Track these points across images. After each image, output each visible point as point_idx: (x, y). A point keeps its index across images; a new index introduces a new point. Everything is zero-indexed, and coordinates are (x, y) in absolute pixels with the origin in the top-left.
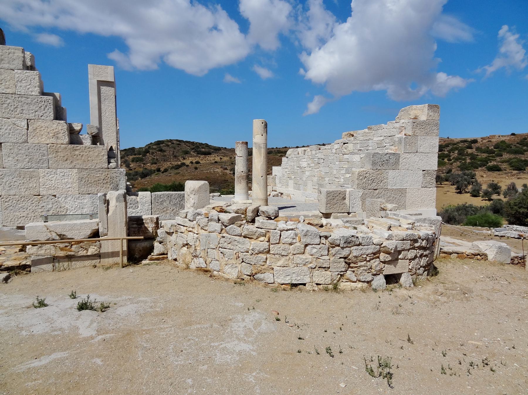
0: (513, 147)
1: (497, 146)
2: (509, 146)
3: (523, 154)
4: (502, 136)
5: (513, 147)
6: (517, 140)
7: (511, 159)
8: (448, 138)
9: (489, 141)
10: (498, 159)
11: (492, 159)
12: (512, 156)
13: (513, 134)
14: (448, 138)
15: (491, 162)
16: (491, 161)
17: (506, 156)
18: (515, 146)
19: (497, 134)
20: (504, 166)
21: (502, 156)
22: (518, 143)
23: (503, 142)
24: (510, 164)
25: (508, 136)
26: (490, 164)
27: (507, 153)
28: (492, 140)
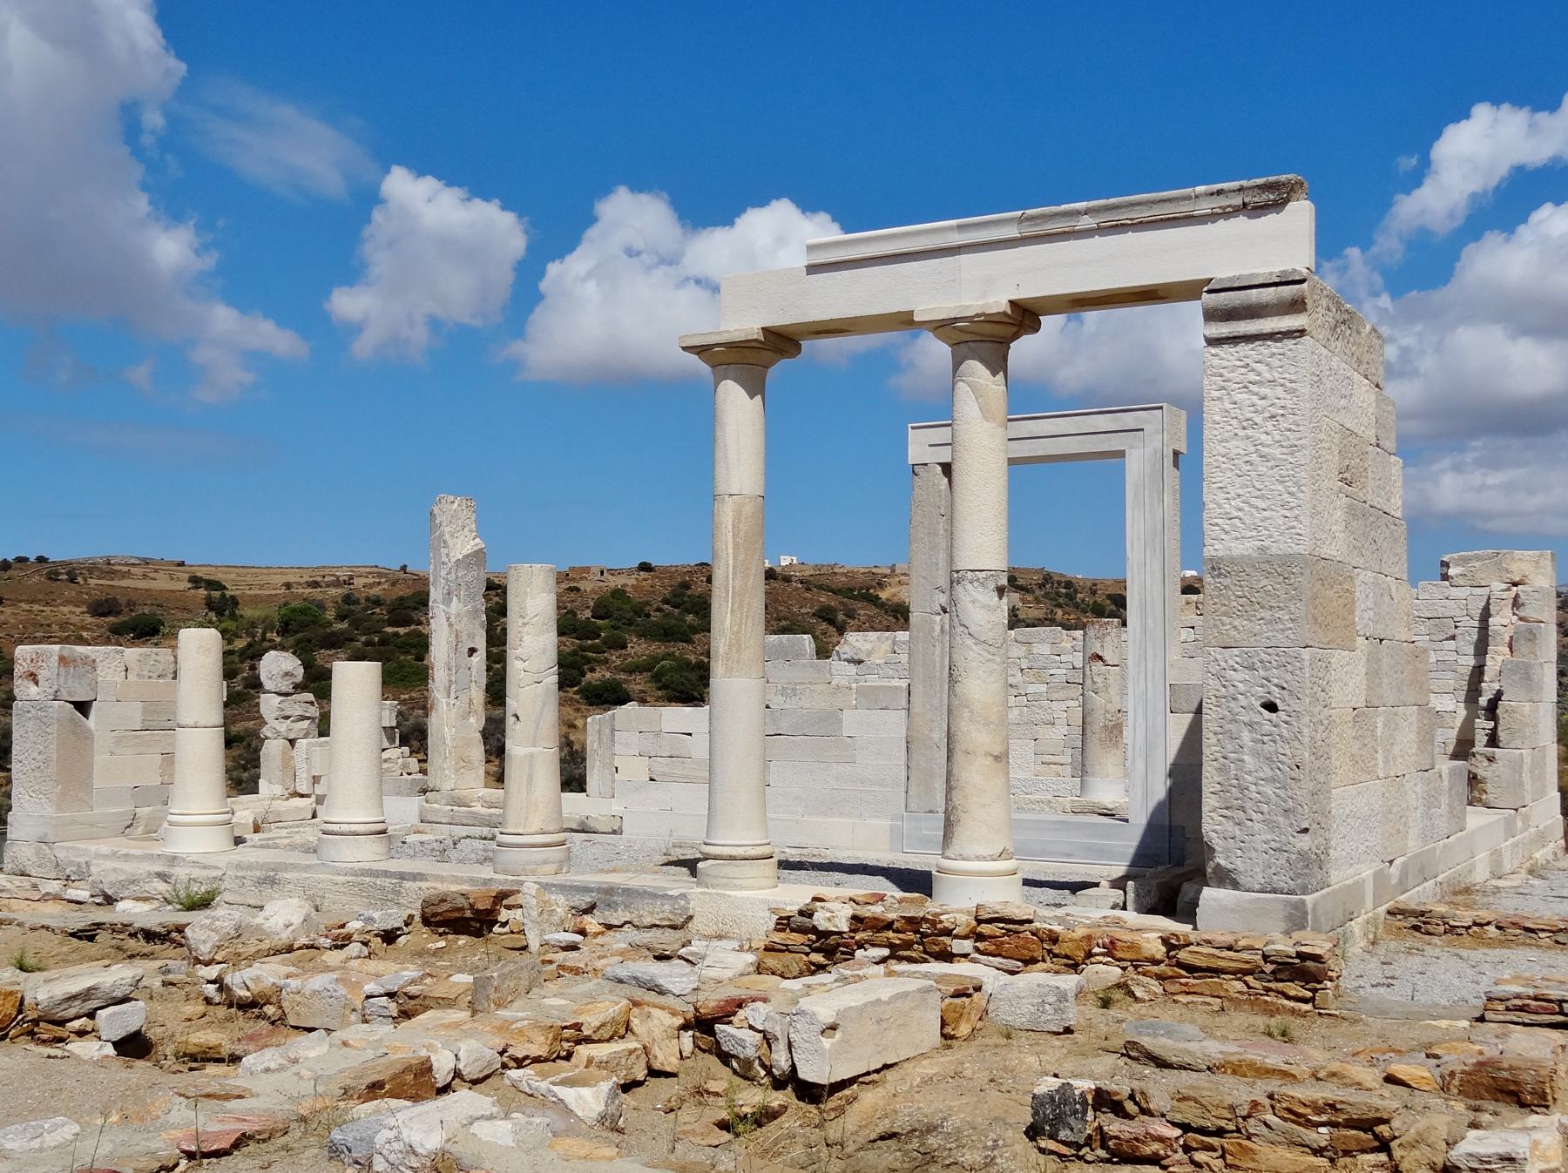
0: (655, 617)
1: (601, 610)
2: (640, 610)
3: (689, 641)
4: (612, 572)
5: (655, 617)
6: (663, 588)
7: (655, 659)
8: (404, 568)
9: (571, 589)
10: (614, 657)
11: (595, 660)
12: (657, 648)
13: (645, 567)
14: (404, 568)
15: (592, 670)
16: (592, 665)
17: (639, 648)
18: (659, 610)
19: (596, 561)
20: (637, 683)
21: (624, 647)
22: (666, 601)
23: (618, 593)
24: (656, 678)
25: (630, 572)
26: (594, 677)
27: (639, 636)
28: (582, 585)
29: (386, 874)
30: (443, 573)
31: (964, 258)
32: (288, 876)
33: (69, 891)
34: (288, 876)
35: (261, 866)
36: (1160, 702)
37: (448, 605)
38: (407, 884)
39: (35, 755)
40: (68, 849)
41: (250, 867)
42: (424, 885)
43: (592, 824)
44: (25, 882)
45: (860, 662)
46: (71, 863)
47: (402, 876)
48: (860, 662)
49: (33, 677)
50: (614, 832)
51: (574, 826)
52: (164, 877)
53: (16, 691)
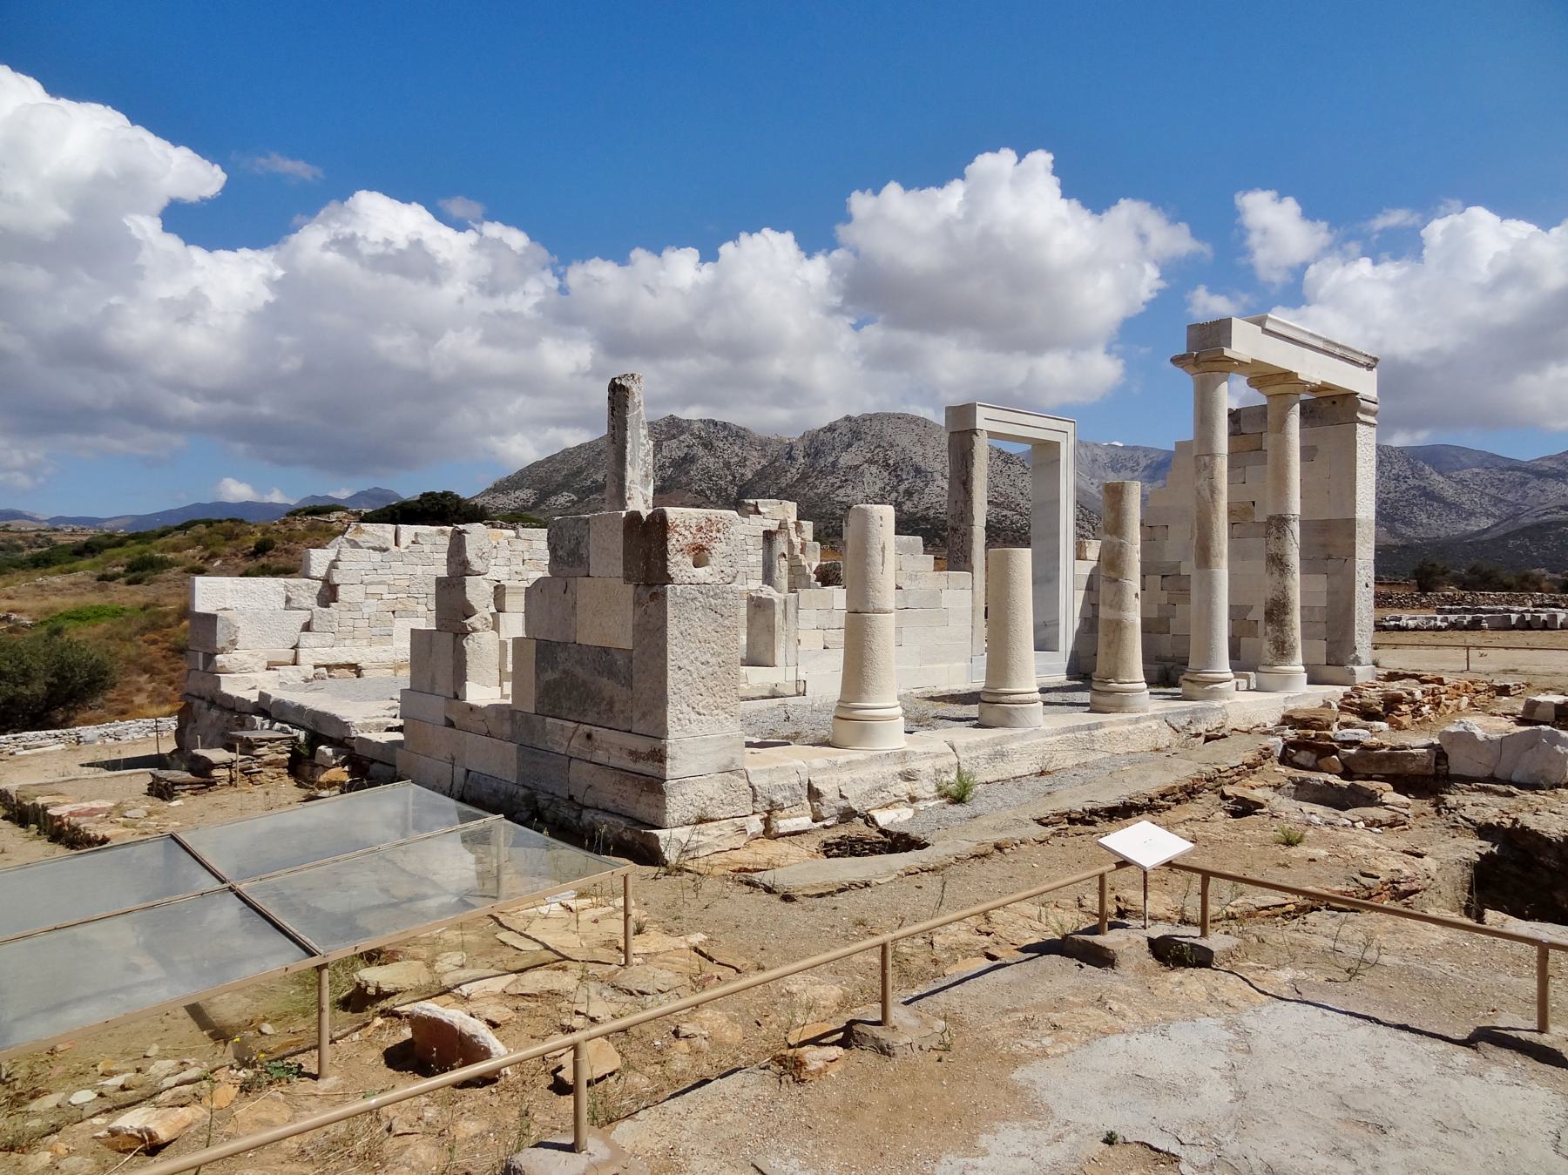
29: (1079, 728)
30: (641, 454)
31: (1307, 350)
32: (1015, 746)
33: (781, 823)
34: (1015, 746)
35: (987, 744)
36: (1070, 586)
37: (646, 487)
38: (1095, 733)
39: (707, 657)
40: (770, 771)
41: (978, 746)
42: (1106, 730)
43: (780, 690)
44: (727, 828)
45: (386, 550)
46: (781, 788)
47: (1089, 728)
48: (386, 550)
49: (700, 555)
50: (798, 694)
51: (766, 694)
52: (908, 777)
53: (672, 570)
